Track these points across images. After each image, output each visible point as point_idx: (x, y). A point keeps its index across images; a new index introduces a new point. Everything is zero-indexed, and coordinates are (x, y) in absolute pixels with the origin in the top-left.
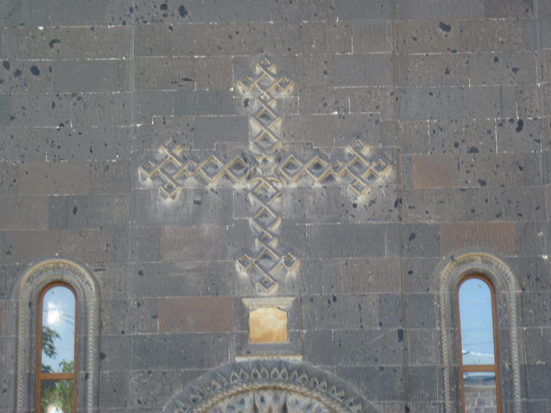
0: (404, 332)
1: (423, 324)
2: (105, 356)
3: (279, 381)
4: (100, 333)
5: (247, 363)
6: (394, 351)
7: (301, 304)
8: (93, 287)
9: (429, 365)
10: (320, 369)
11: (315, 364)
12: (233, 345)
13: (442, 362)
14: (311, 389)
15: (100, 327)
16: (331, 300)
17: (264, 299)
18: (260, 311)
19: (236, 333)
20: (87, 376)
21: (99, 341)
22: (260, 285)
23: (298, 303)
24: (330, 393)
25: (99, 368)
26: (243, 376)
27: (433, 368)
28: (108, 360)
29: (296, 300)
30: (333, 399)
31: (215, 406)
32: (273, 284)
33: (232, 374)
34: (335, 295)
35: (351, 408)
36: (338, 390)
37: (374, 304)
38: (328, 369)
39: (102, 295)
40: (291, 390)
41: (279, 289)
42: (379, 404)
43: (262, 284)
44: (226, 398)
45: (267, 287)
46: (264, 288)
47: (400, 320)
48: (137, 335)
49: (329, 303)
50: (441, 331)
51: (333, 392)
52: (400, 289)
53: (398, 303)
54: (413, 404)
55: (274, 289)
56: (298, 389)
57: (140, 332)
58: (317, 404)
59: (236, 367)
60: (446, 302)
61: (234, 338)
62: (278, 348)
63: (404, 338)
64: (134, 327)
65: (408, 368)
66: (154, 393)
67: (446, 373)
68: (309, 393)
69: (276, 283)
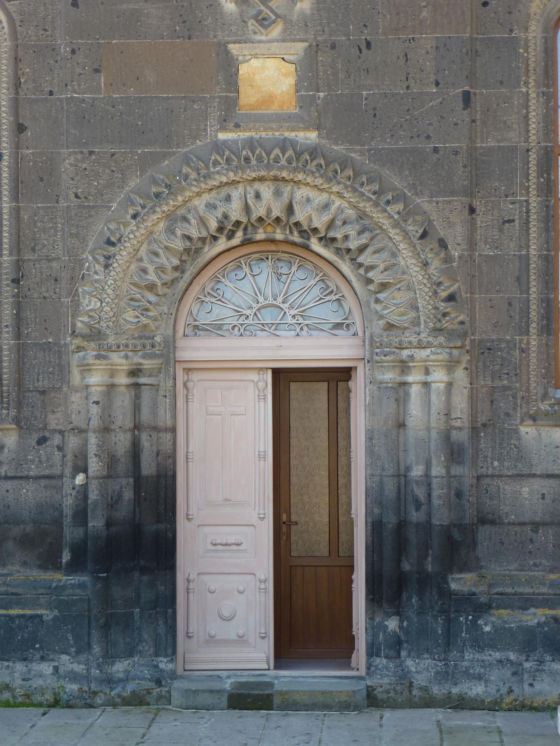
0: (472, 95)
1: (501, 82)
3: (281, 168)
4: (17, 93)
5: (235, 142)
6: (456, 124)
7: (317, 52)
8: (5, 24)
9: (507, 144)
10: (344, 151)
11: (336, 144)
12: (214, 114)
13: (527, 141)
14: (329, 180)
16: (363, 47)
17: (261, 45)
18: (255, 63)
19: (220, 97)
22: (255, 23)
23: (314, 50)
24: (357, 186)
25: (17, 146)
26: (228, 160)
27: (513, 149)
28: (29, 134)
29: (310, 46)
30: (363, 194)
31: (188, 204)
32: (274, 22)
33: (213, 158)
35: (388, 208)
36: (370, 181)
37: (427, 53)
38: (355, 152)
39: (19, 37)
41: (284, 31)
42: (430, 202)
43: (257, 21)
44: (204, 192)
45: (265, 27)
46: (261, 28)
47: (467, 77)
48: (72, 97)
50: (528, 94)
51: (363, 184)
52: (469, 29)
53: (464, 50)
54: (480, 202)
55: (276, 31)
57: (75, 92)
58: (338, 202)
59: (219, 147)
60: (538, 49)
61: (216, 104)
62: (282, 119)
63: (472, 105)
64: (66, 86)
65: (476, 148)
66: (98, 183)
67: (533, 156)
68: (325, 186)
69: (279, 20)
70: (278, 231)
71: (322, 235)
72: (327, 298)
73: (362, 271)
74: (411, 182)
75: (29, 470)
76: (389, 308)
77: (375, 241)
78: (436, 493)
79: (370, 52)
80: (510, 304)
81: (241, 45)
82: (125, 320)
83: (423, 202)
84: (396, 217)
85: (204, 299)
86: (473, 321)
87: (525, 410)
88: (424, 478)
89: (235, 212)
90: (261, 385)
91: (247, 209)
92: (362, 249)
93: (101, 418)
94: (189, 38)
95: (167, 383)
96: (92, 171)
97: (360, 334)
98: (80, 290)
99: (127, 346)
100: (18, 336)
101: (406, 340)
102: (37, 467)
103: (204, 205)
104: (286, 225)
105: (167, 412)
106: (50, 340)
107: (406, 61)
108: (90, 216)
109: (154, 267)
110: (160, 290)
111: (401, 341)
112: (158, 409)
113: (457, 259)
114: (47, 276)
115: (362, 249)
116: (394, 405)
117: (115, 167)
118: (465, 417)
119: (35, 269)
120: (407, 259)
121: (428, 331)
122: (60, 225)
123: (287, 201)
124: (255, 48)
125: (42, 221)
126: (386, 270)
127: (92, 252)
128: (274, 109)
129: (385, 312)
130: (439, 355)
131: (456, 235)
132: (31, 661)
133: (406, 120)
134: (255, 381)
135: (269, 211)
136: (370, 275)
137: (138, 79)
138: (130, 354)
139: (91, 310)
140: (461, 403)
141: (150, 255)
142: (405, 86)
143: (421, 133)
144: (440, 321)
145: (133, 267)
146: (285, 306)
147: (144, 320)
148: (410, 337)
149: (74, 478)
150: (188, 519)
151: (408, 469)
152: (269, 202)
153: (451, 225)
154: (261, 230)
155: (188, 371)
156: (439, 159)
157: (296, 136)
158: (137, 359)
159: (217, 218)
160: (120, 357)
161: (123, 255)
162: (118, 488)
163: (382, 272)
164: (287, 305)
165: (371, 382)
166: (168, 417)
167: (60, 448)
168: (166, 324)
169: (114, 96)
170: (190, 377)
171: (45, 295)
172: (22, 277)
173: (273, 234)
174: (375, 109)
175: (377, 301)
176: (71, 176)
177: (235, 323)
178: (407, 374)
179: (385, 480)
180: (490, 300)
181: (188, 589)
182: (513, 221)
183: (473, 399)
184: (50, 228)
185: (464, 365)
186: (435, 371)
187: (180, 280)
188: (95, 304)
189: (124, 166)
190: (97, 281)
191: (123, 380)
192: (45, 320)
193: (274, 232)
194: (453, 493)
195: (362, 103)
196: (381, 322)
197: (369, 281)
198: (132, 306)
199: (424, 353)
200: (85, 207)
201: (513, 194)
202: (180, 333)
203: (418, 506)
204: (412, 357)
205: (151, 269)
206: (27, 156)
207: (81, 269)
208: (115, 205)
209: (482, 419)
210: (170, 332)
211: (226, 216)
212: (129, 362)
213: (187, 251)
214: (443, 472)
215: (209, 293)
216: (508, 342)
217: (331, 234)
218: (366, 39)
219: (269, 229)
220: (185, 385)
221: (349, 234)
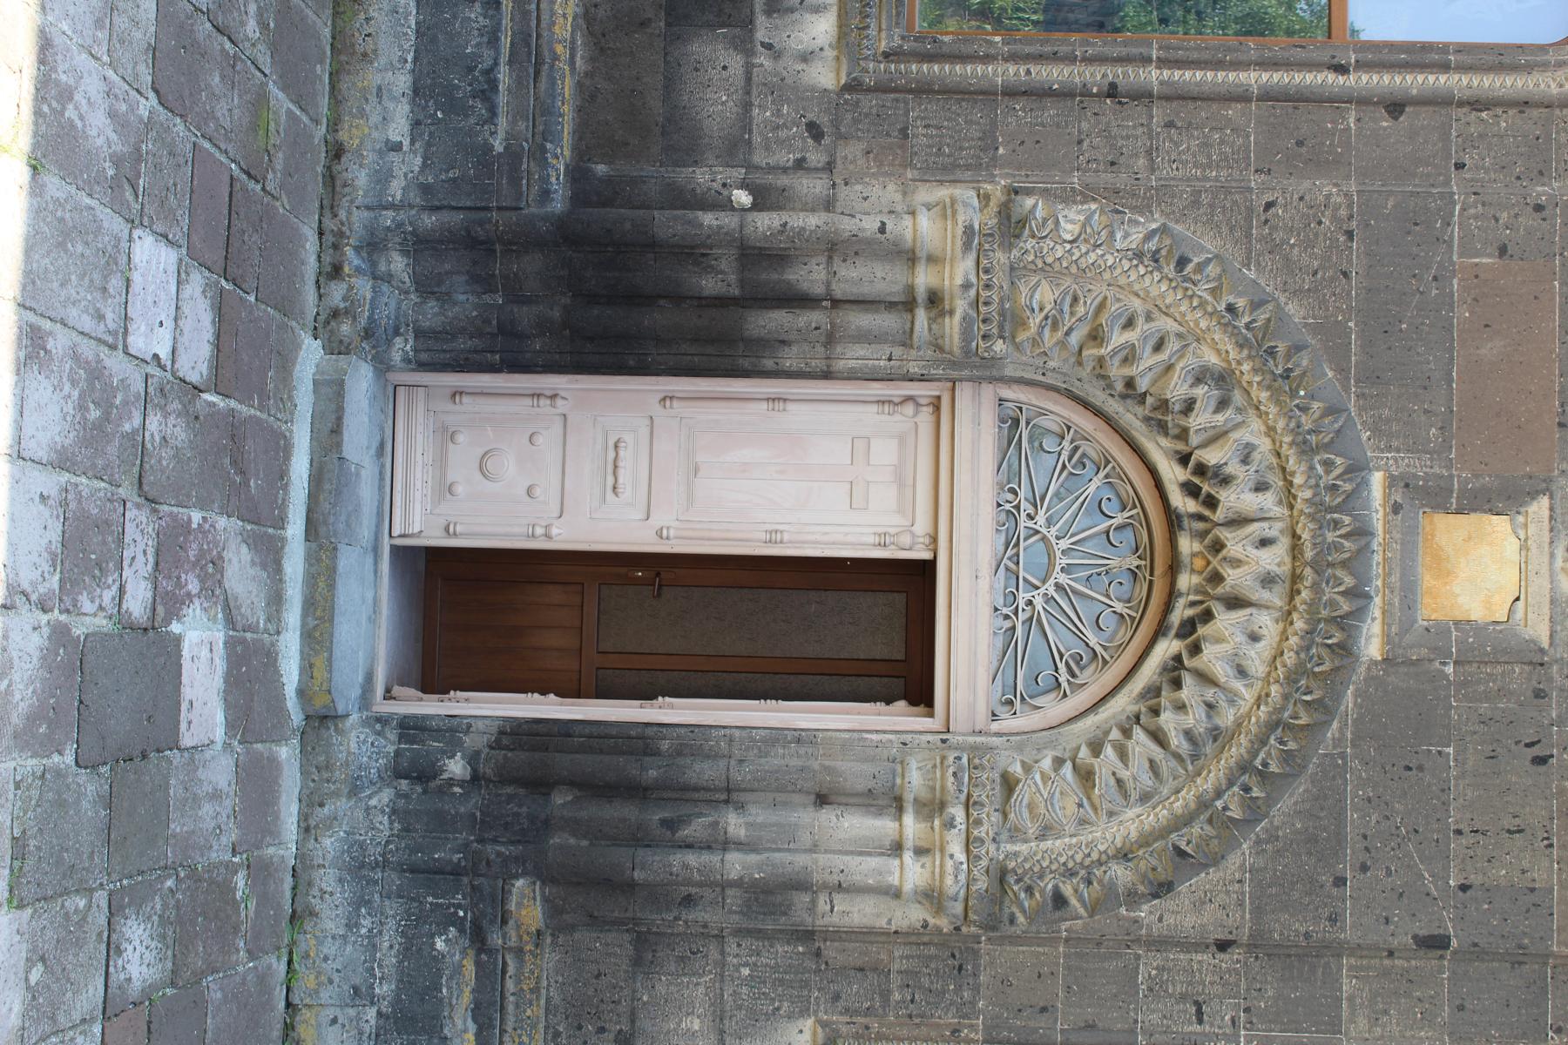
0: (1440, 952)
1: (1461, 1008)
2: (1396, 119)
3: (1315, 587)
4: (1461, 104)
6: (1387, 921)
7: (1531, 663)
10: (1342, 708)
12: (1419, 466)
14: (1292, 678)
15: (1477, 104)
16: (1536, 751)
17: (1546, 559)
18: (1512, 546)
19: (1451, 476)
20: (1341, 69)
21: (1441, 101)
23: (1536, 659)
25: (1363, 101)
29: (1542, 650)
31: (1252, 412)
33: (1339, 461)
35: (1236, 789)
36: (1287, 757)
37: (1523, 872)
38: (1341, 729)
44: (1274, 441)
47: (1476, 945)
48: (1454, 203)
54: (1238, 961)
56: (1294, 641)
57: (1463, 209)
58: (1248, 695)
59: (1357, 470)
61: (1437, 470)
62: (1408, 592)
63: (1422, 953)
65: (1340, 956)
66: (1293, 246)
68: (1281, 671)
70: (1196, 579)
71: (1186, 662)
72: (1062, 666)
73: (1115, 734)
75: (762, 107)
76: (1045, 783)
77: (1173, 763)
78: (692, 859)
80: (1044, 1010)
82: (1038, 284)
84: (1219, 804)
85: (1068, 438)
86: (1014, 940)
87: (844, 1029)
88: (721, 838)
89: (1236, 499)
92: (1158, 737)
94: (1561, 425)
96: (1316, 235)
97: (995, 727)
98: (1094, 206)
99: (987, 286)
100: (1011, 92)
102: (765, 121)
103: (1245, 440)
104: (1206, 593)
106: (1001, 151)
107: (1509, 831)
110: (1090, 352)
111: (983, 805)
115: (1158, 737)
116: (861, 785)
117: (1323, 278)
118: (835, 919)
119: (1134, 127)
120: (1134, 822)
123: (1254, 597)
124: (1539, 547)
125: (1222, 142)
126: (1119, 782)
127: (1164, 230)
128: (1427, 580)
129: (1038, 777)
131: (1180, 913)
132: (413, 102)
135: (1236, 563)
136: (1109, 751)
138: (973, 292)
139: (1057, 222)
140: (859, 912)
141: (1157, 336)
142: (1461, 827)
144: (1018, 881)
145: (1137, 304)
147: (1035, 321)
148: (990, 822)
149: (743, 185)
150: (664, 399)
151: (740, 807)
152: (1253, 561)
153: (1198, 905)
154: (1197, 547)
155: (936, 404)
157: (1373, 619)
158: (961, 306)
161: (1157, 286)
162: (724, 265)
164: (1052, 591)
166: (852, 363)
167: (800, 164)
169: (1455, 281)
174: (1421, 768)
175: (1058, 762)
176: (1307, 198)
177: (1022, 495)
178: (917, 813)
179: (722, 763)
181: (539, 395)
182: (1200, 1021)
183: (867, 935)
184: (1209, 156)
185: (931, 921)
186: (923, 866)
188: (1069, 230)
190: (1112, 234)
191: (923, 279)
193: (1193, 571)
194: (693, 890)
196: (1017, 769)
197: (1096, 748)
199: (957, 849)
200: (1249, 219)
202: (1006, 393)
203: (670, 825)
204: (950, 824)
205: (1131, 336)
206: (1344, 118)
207: (1133, 209)
208: (1252, 275)
209: (830, 950)
210: (1009, 371)
211: (1226, 481)
213: (1163, 405)
214: (733, 876)
215: (1076, 448)
216: (973, 1003)
217: (1188, 680)
219: (1199, 563)
221: (1187, 713)
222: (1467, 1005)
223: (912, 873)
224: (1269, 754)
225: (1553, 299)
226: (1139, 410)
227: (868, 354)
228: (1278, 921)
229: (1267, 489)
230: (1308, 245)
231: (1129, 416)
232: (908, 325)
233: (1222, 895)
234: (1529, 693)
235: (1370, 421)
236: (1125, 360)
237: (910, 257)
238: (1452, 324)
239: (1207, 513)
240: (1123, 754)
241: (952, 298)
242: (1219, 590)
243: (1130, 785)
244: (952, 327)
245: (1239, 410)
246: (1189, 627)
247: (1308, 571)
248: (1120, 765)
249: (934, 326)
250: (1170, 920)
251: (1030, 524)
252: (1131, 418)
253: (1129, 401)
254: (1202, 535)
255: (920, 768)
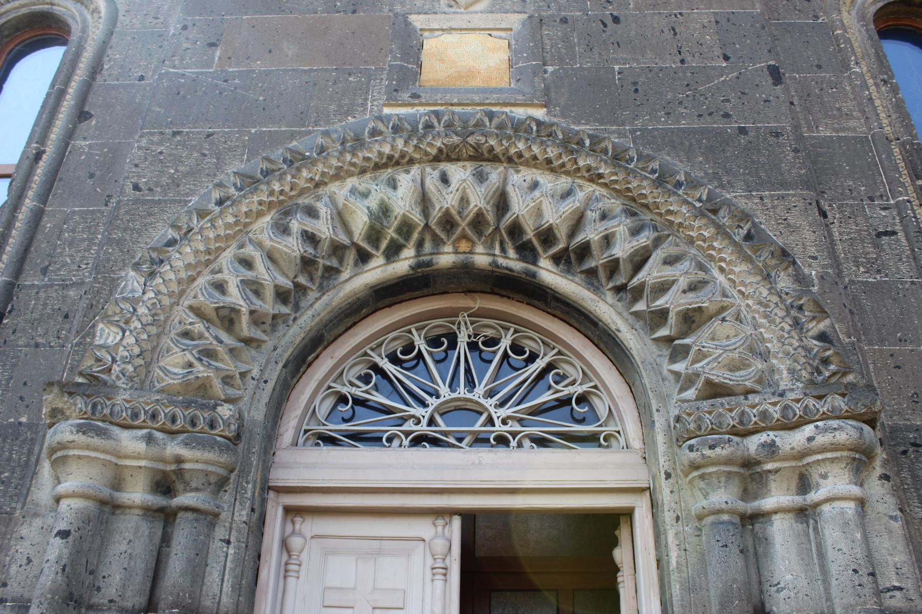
16: (609, 22)
23: (537, 23)
25: (69, 135)
28: (94, 123)
29: (529, 17)
34: (615, 13)
37: (704, 27)
39: (119, 25)
40: (520, 155)
42: (749, 197)
49: (605, 25)
57: (174, 67)
66: (176, 171)
70: (480, 249)
71: (562, 245)
74: (710, 171)
76: (705, 357)
79: (619, 26)
81: (428, 16)
83: (735, 197)
90: (440, 545)
91: (424, 201)
92: (640, 261)
93: (64, 570)
94: (354, 12)
95: (236, 514)
97: (637, 444)
99: (154, 416)
101: (754, 411)
105: (226, 578)
106: (24, 419)
107: (675, 34)
108: (150, 215)
109: (239, 279)
111: (743, 413)
112: (208, 569)
113: (816, 281)
114: (53, 310)
115: (640, 261)
116: (737, 561)
117: (209, 150)
119: (37, 299)
121: (800, 385)
122: (100, 236)
128: (477, 83)
130: (837, 433)
131: (805, 240)
133: (687, 96)
134: (427, 540)
135: (464, 201)
136: (661, 302)
137: (270, 51)
138: (159, 435)
141: (237, 265)
143: (713, 110)
144: (820, 373)
145: (201, 281)
146: (490, 403)
153: (793, 229)
154: (448, 248)
155: (291, 512)
156: (750, 142)
159: (368, 208)
160: (137, 438)
163: (684, 292)
165: (678, 518)
168: (252, 398)
170: (297, 526)
171: (40, 340)
172: (10, 312)
173: (470, 256)
174: (635, 83)
176: (137, 162)
178: (756, 497)
180: (892, 355)
182: (894, 233)
184: (84, 240)
186: (824, 476)
187: (291, 322)
189: (225, 148)
191: (137, 494)
192: (25, 384)
193: (471, 252)
195: (614, 78)
198: (183, 344)
199: (797, 439)
200: (144, 202)
201: (881, 196)
204: (771, 449)
211: (385, 210)
212: (154, 451)
213: (307, 263)
215: (352, 384)
218: (612, 14)
219: (464, 246)
220: (285, 545)
222: (816, 62)
223: (834, 483)
224: (643, 169)
225: (256, 19)
226: (312, 295)
227: (219, 567)
228: (789, 171)
229: (394, 180)
230: (178, 160)
231: (317, 306)
232: (190, 515)
233: (778, 211)
234: (564, 26)
235: (339, 117)
236: (257, 293)
237: (108, 508)
238: (265, 71)
239: (415, 236)
240: (663, 288)
241: (163, 460)
242: (490, 217)
243: (693, 278)
244: (196, 459)
245: (319, 198)
246: (527, 253)
247: (471, 140)
248: (674, 288)
249: (194, 485)
250: (812, 251)
251: (424, 422)
252: (319, 307)
253: (303, 304)
254: (437, 242)
255: (706, 496)
